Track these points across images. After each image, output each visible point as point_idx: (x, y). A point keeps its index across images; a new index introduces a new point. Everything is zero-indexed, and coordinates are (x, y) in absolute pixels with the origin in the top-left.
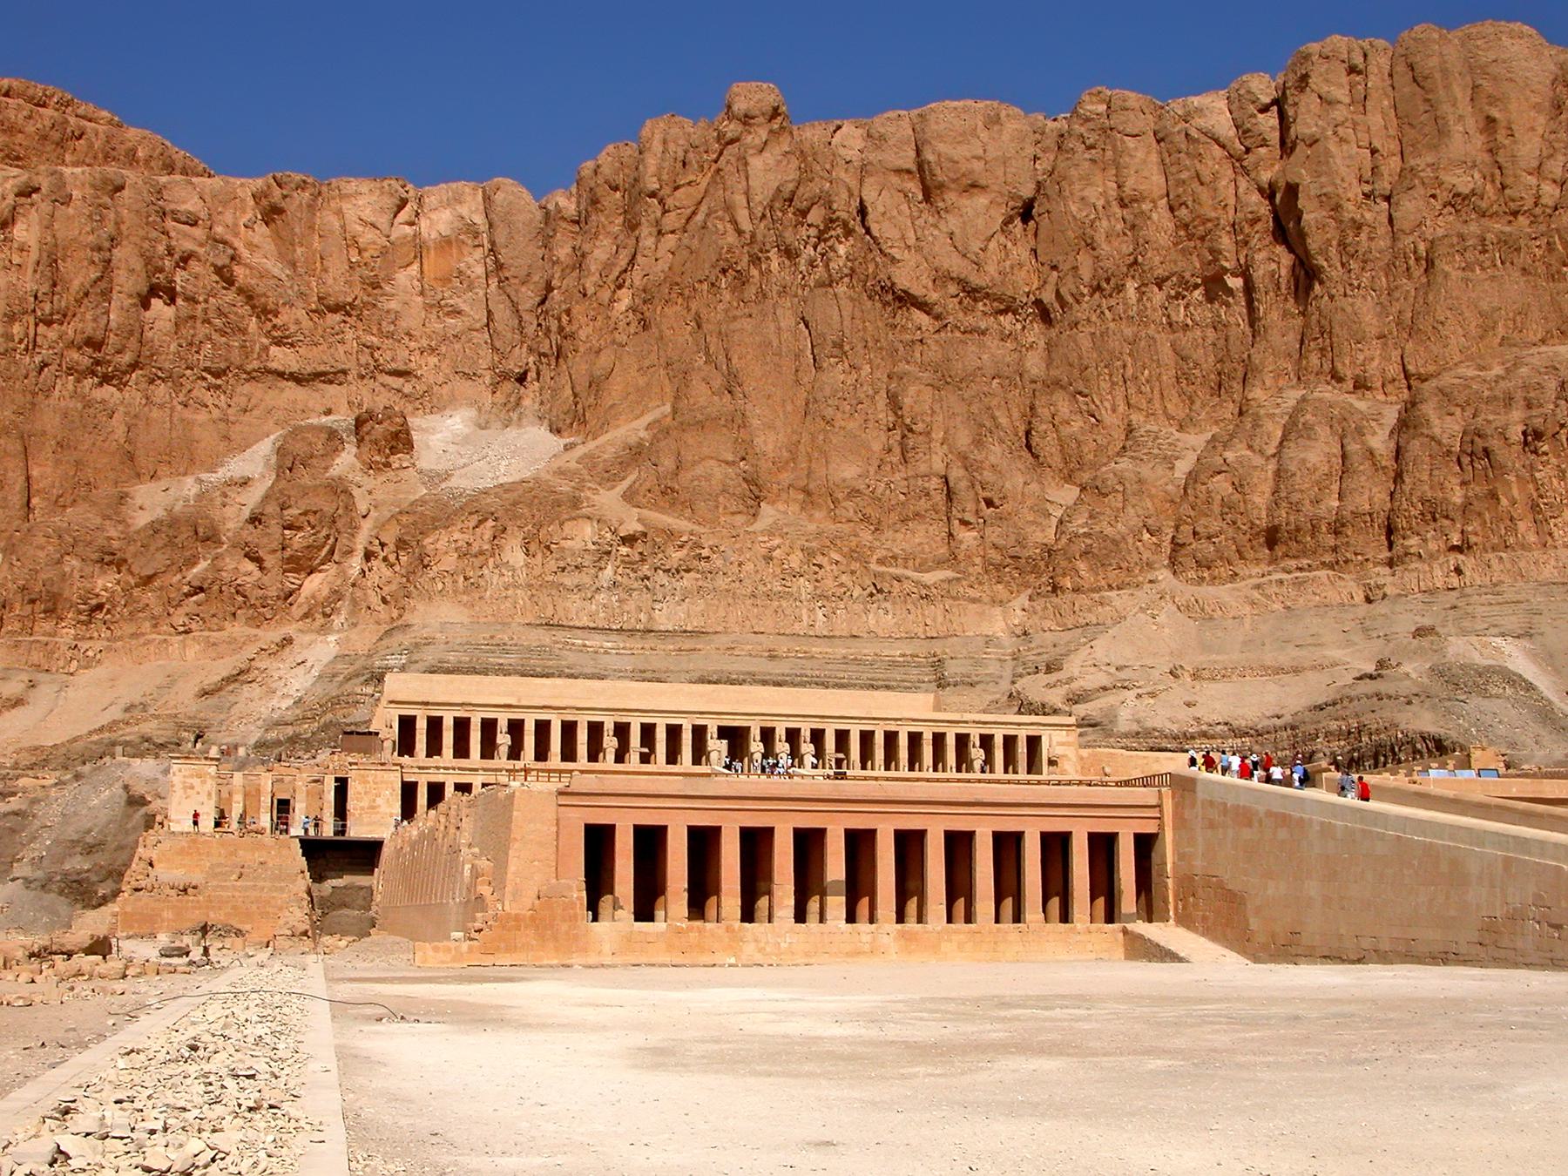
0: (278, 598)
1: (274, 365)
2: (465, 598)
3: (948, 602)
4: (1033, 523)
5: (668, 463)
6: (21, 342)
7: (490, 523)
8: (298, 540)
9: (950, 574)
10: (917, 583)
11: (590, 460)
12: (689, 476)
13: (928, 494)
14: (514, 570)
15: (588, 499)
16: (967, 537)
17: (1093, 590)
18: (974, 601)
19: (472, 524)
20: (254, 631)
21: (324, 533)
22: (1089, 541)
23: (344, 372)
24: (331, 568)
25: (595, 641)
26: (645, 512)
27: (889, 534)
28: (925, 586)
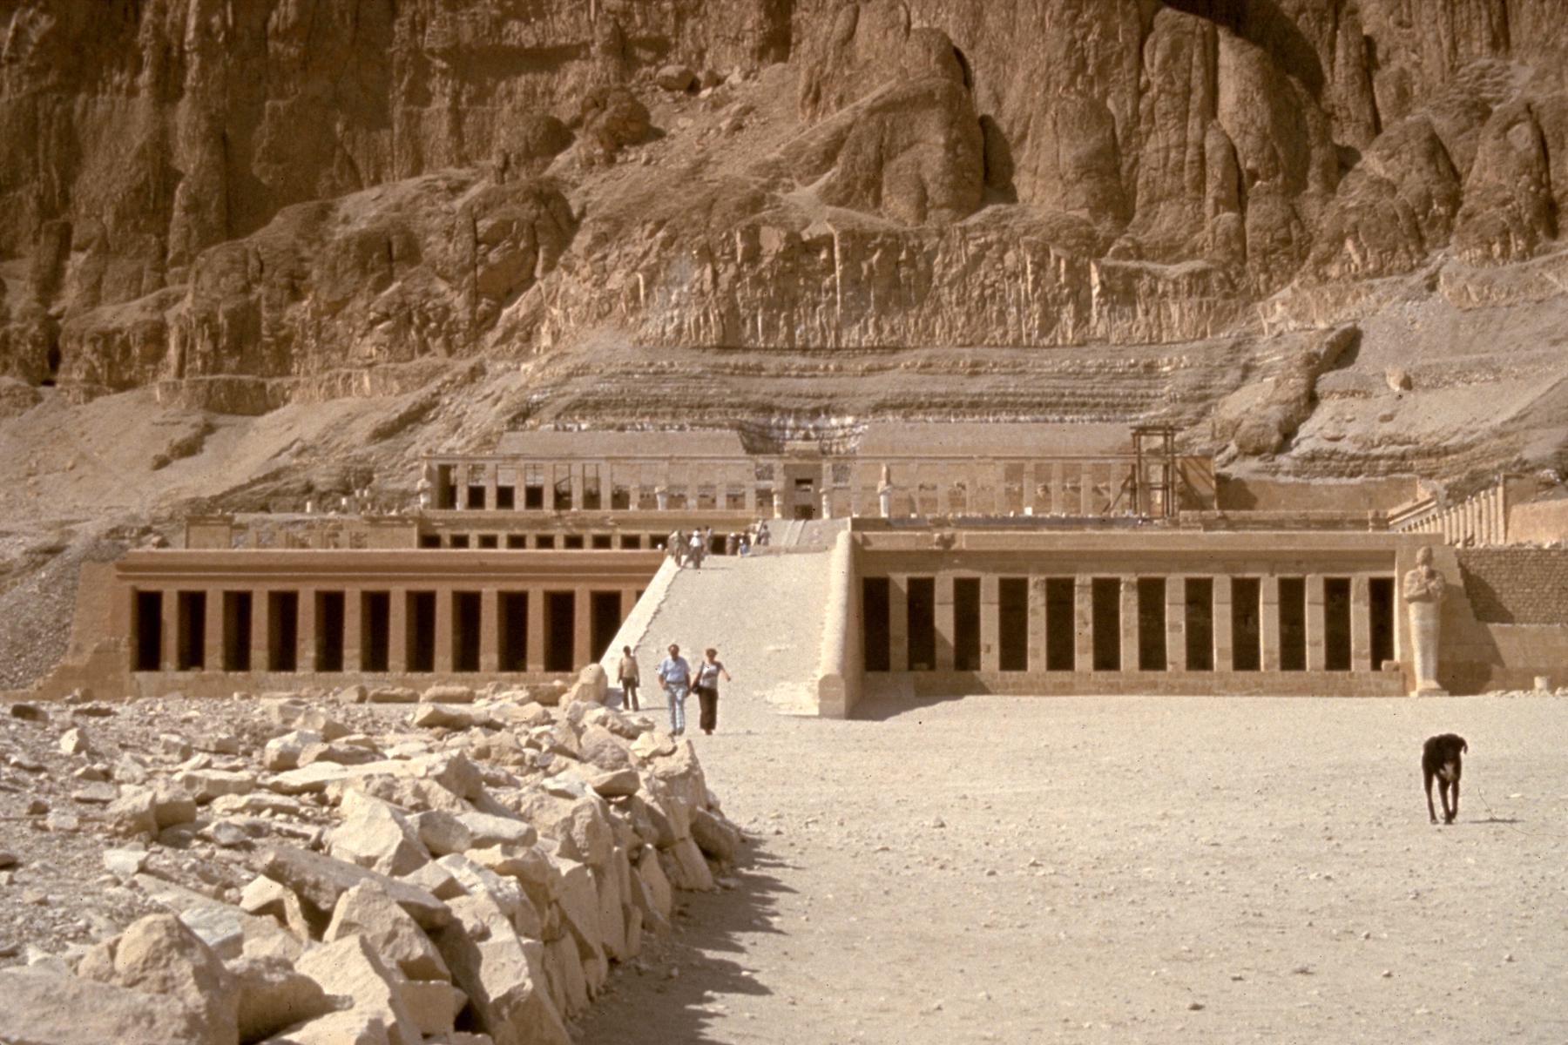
0: (472, 321)
1: (509, 41)
2: (631, 320)
3: (1195, 299)
4: (1312, 195)
5: (870, 149)
6: (219, 32)
7: (661, 234)
8: (493, 257)
9: (1198, 264)
10: (1156, 278)
11: (796, 152)
12: (894, 165)
13: (1182, 169)
14: (681, 284)
15: (773, 198)
16: (1228, 217)
17: (1355, 278)
18: (1227, 296)
19: (646, 233)
20: (450, 361)
21: (522, 245)
22: (1352, 218)
23: (586, 45)
24: (535, 287)
25: (773, 363)
26: (842, 210)
27: (1137, 217)
28: (1167, 281)
